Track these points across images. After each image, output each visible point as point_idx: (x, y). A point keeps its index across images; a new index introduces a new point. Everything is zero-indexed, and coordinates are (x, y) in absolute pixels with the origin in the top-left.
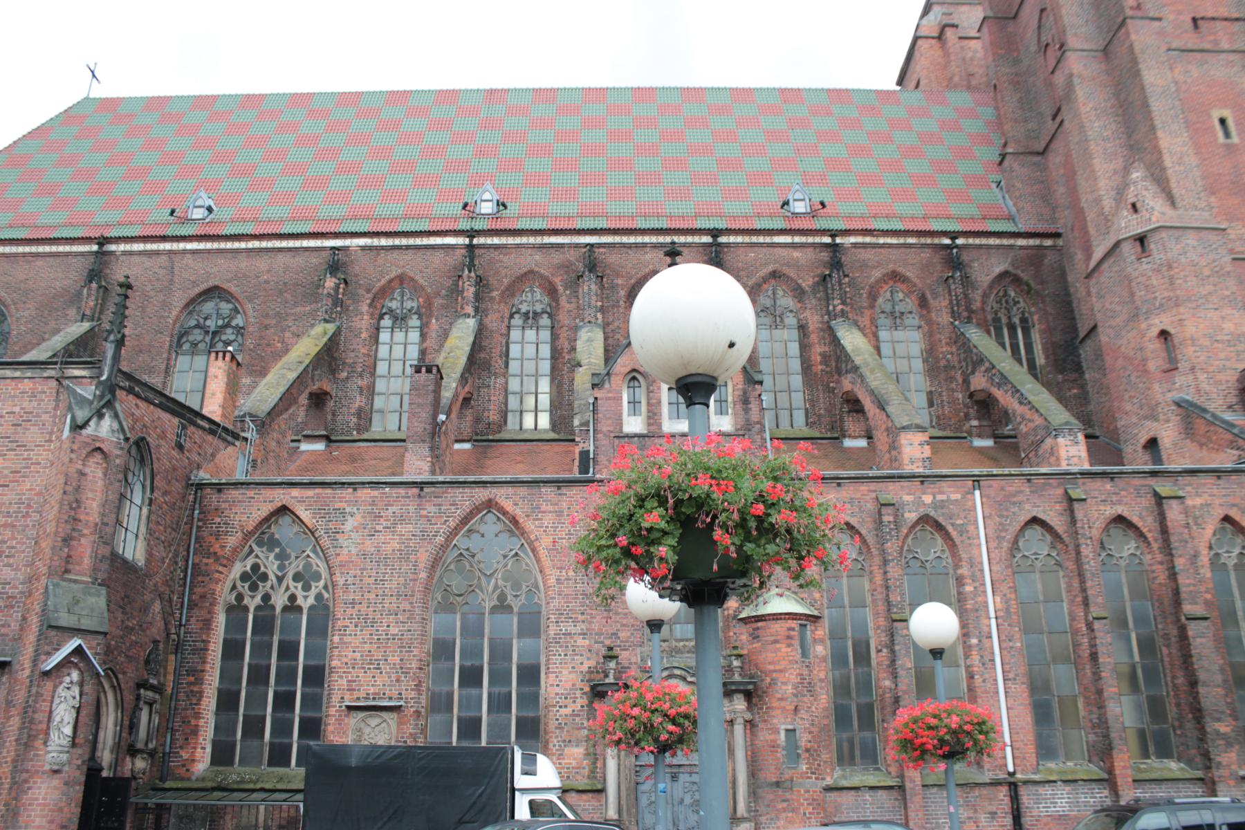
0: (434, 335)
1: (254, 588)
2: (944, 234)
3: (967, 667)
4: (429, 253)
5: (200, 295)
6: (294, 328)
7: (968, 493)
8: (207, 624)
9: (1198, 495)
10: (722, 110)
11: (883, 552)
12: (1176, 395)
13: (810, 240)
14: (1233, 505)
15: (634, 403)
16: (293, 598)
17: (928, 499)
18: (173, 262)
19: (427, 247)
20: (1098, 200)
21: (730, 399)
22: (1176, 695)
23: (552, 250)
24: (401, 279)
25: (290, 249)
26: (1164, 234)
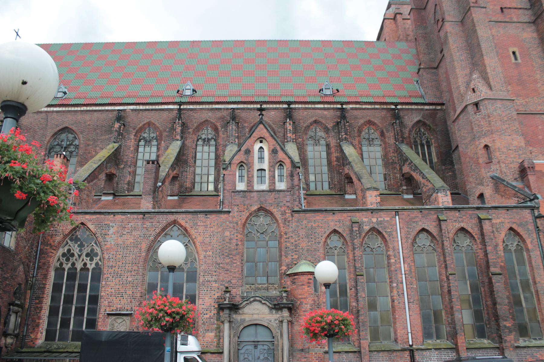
0: (163, 149)
1: (68, 260)
2: (392, 103)
3: (392, 297)
4: (162, 112)
5: (59, 131)
6: (101, 146)
7: (393, 217)
8: (45, 277)
9: (498, 218)
10: (295, 50)
11: (353, 244)
12: (491, 174)
13: (332, 106)
14: (514, 223)
15: (241, 176)
16: (85, 264)
17: (374, 220)
18: (47, 117)
19: (160, 110)
20: (458, 87)
21: (285, 175)
22: (487, 310)
23: (216, 111)
24: (149, 124)
25: (100, 111)
26: (486, 102)
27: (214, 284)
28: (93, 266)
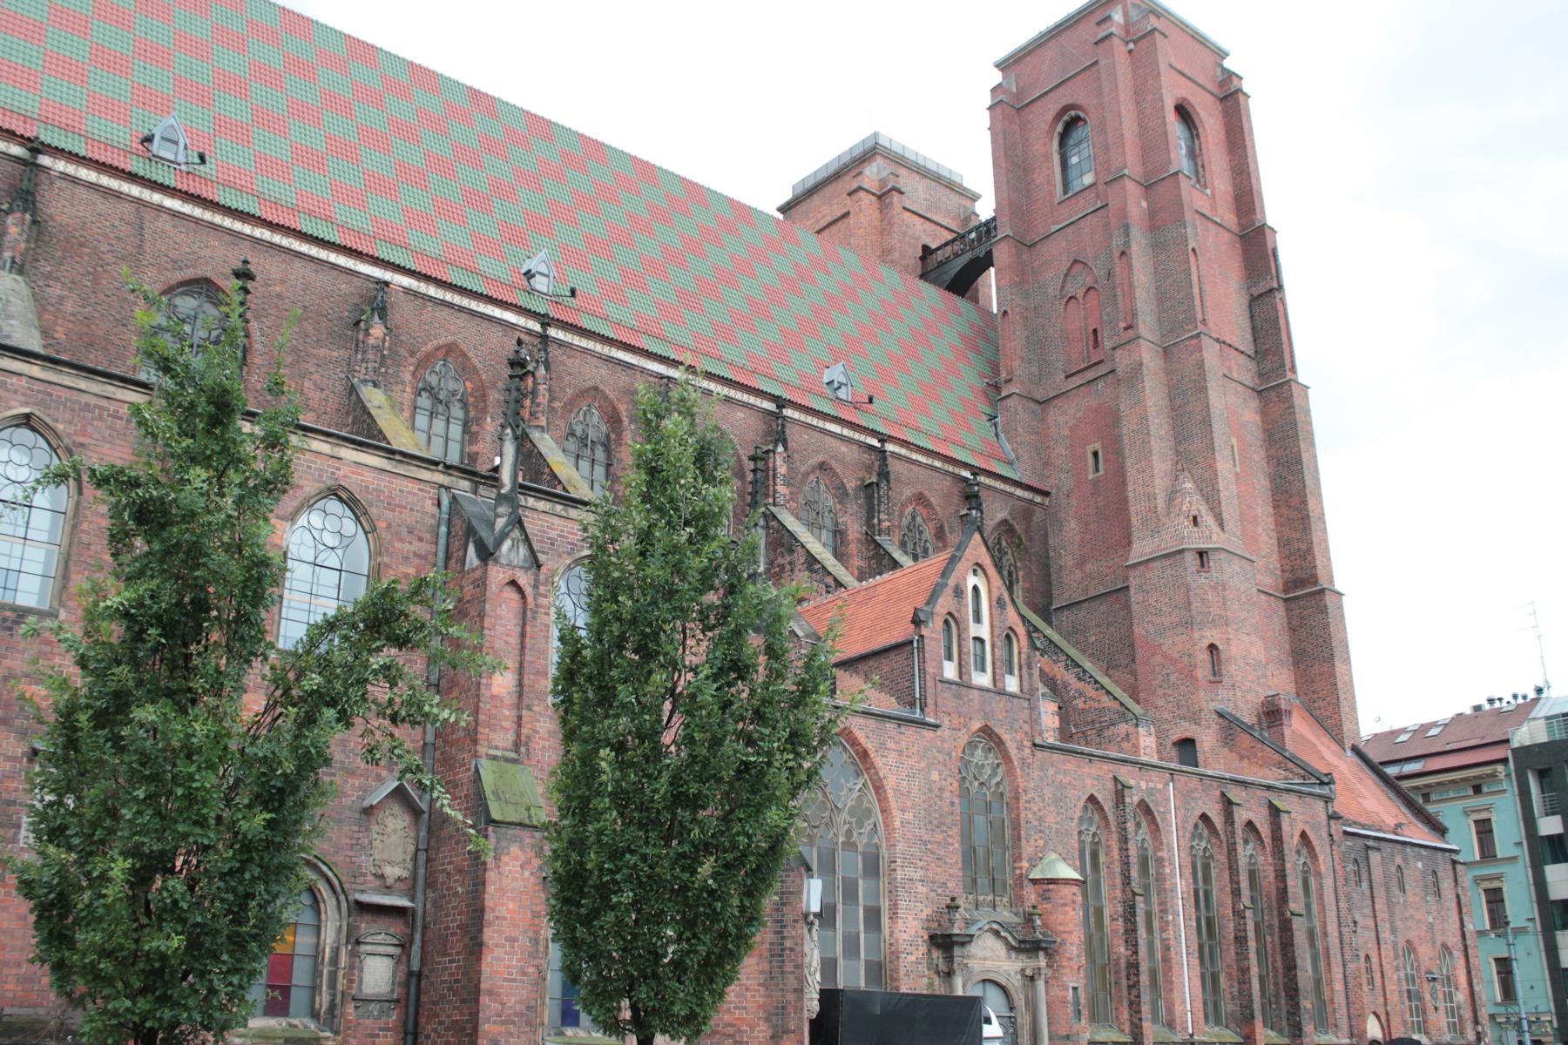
0: (488, 438)
3: (1162, 940)
4: (485, 324)
5: (181, 284)
6: (316, 377)
12: (1219, 707)
13: (857, 436)
18: (141, 219)
19: (483, 316)
20: (1151, 497)
22: (1275, 976)
23: (619, 368)
24: (450, 349)
25: (312, 259)
26: (1223, 555)
27: (921, 889)
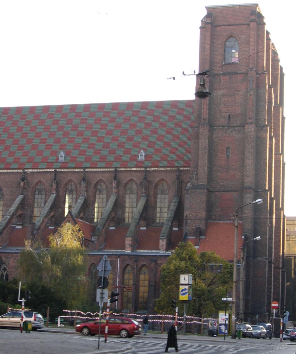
9: (161, 261)
16: (2, 273)
28: (5, 274)
